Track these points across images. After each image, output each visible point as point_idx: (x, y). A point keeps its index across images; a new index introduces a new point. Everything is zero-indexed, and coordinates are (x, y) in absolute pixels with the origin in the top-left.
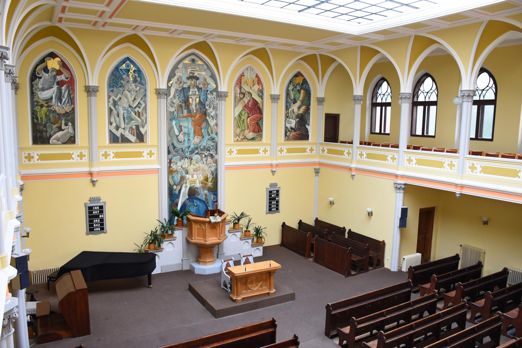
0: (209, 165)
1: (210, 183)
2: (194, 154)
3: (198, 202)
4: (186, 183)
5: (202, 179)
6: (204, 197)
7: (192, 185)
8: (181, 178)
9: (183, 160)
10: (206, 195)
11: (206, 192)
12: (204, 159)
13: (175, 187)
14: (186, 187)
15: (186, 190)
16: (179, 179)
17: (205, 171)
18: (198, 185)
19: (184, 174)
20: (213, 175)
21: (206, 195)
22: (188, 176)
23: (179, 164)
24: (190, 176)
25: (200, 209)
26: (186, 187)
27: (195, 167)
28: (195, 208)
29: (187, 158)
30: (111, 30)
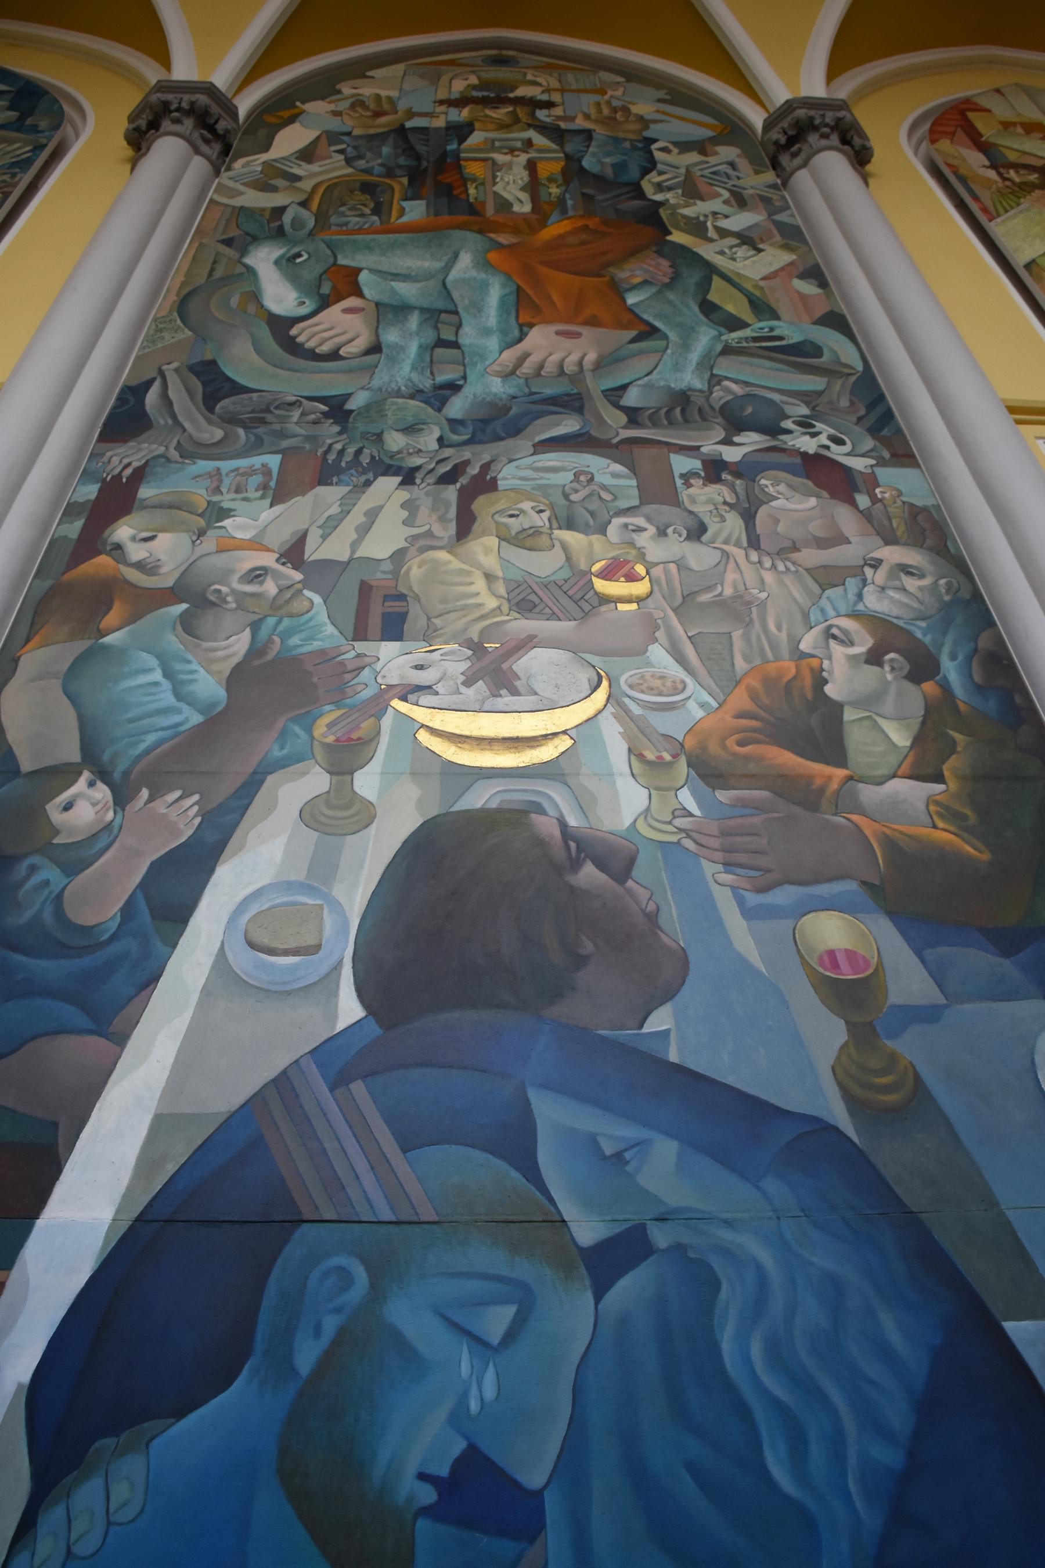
0: (811, 557)
1: (912, 793)
2: (523, 444)
3: (664, 1169)
4: (346, 756)
5: (697, 706)
6: (827, 1034)
7: (479, 798)
8: (237, 678)
9: (331, 495)
10: (851, 993)
11: (831, 931)
12: (703, 497)
13: (83, 807)
14: (338, 816)
15: (322, 872)
16: (209, 687)
17: (739, 609)
18: (625, 804)
19: (320, 625)
20: (922, 667)
21: (851, 993)
22: (392, 660)
23: (254, 521)
24: (449, 662)
25: (740, 1349)
26: (338, 816)
27: (544, 564)
28: (573, 1317)
29: (409, 478)
30: (8, 201)
